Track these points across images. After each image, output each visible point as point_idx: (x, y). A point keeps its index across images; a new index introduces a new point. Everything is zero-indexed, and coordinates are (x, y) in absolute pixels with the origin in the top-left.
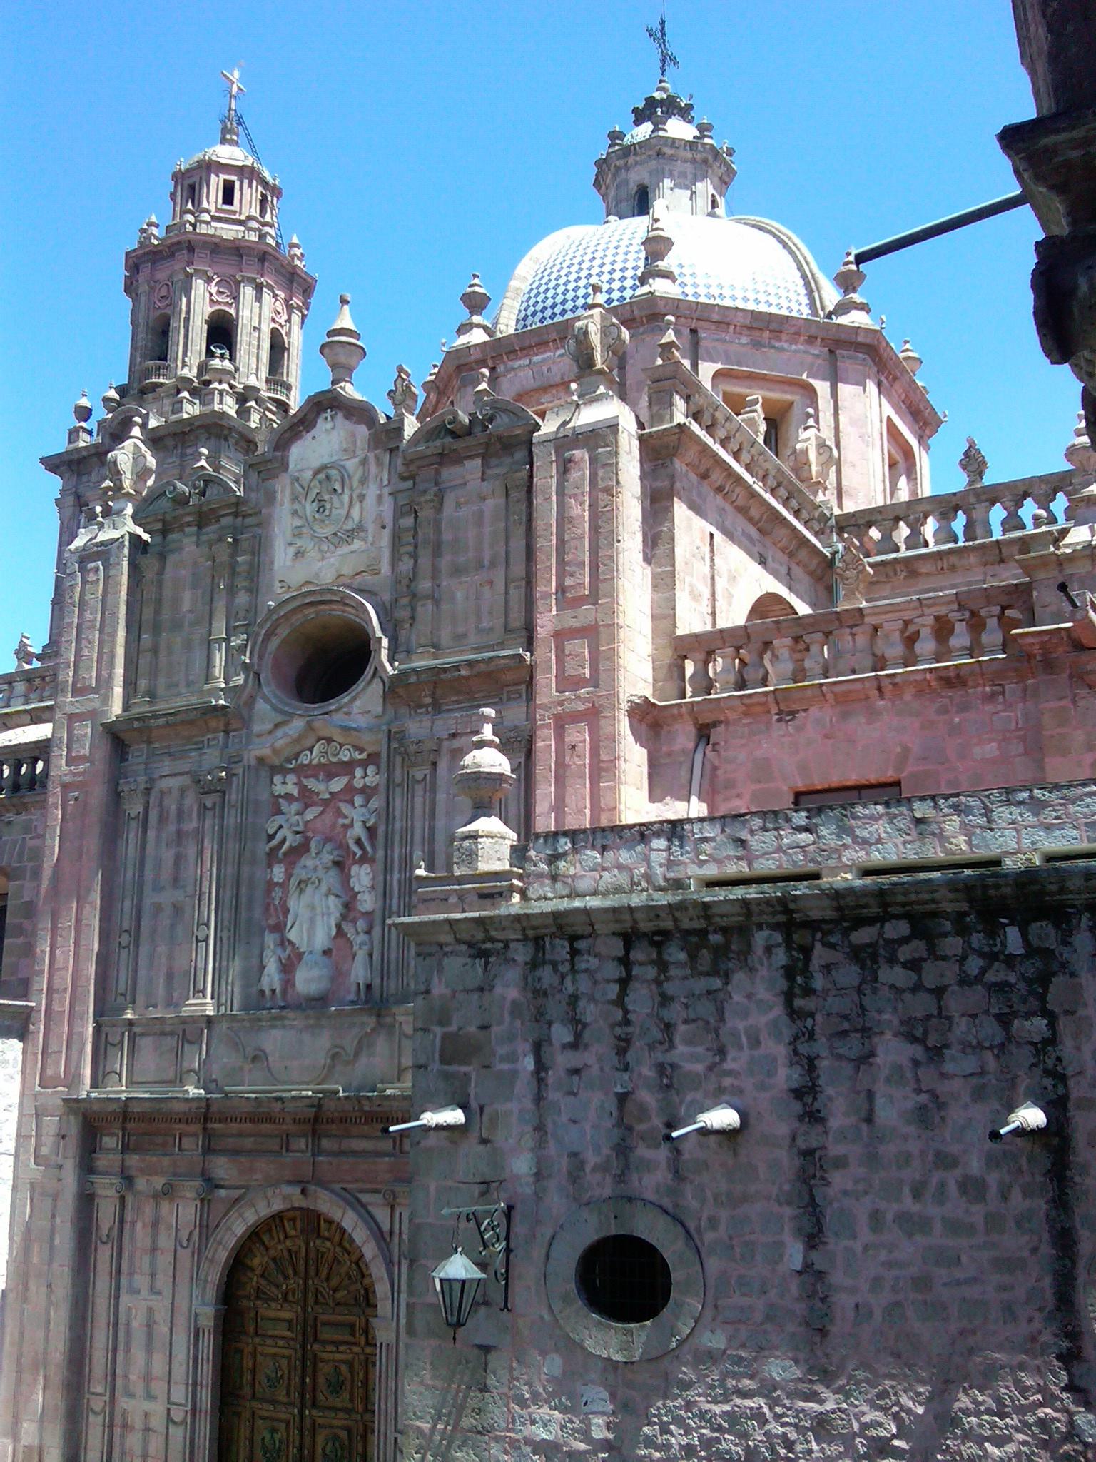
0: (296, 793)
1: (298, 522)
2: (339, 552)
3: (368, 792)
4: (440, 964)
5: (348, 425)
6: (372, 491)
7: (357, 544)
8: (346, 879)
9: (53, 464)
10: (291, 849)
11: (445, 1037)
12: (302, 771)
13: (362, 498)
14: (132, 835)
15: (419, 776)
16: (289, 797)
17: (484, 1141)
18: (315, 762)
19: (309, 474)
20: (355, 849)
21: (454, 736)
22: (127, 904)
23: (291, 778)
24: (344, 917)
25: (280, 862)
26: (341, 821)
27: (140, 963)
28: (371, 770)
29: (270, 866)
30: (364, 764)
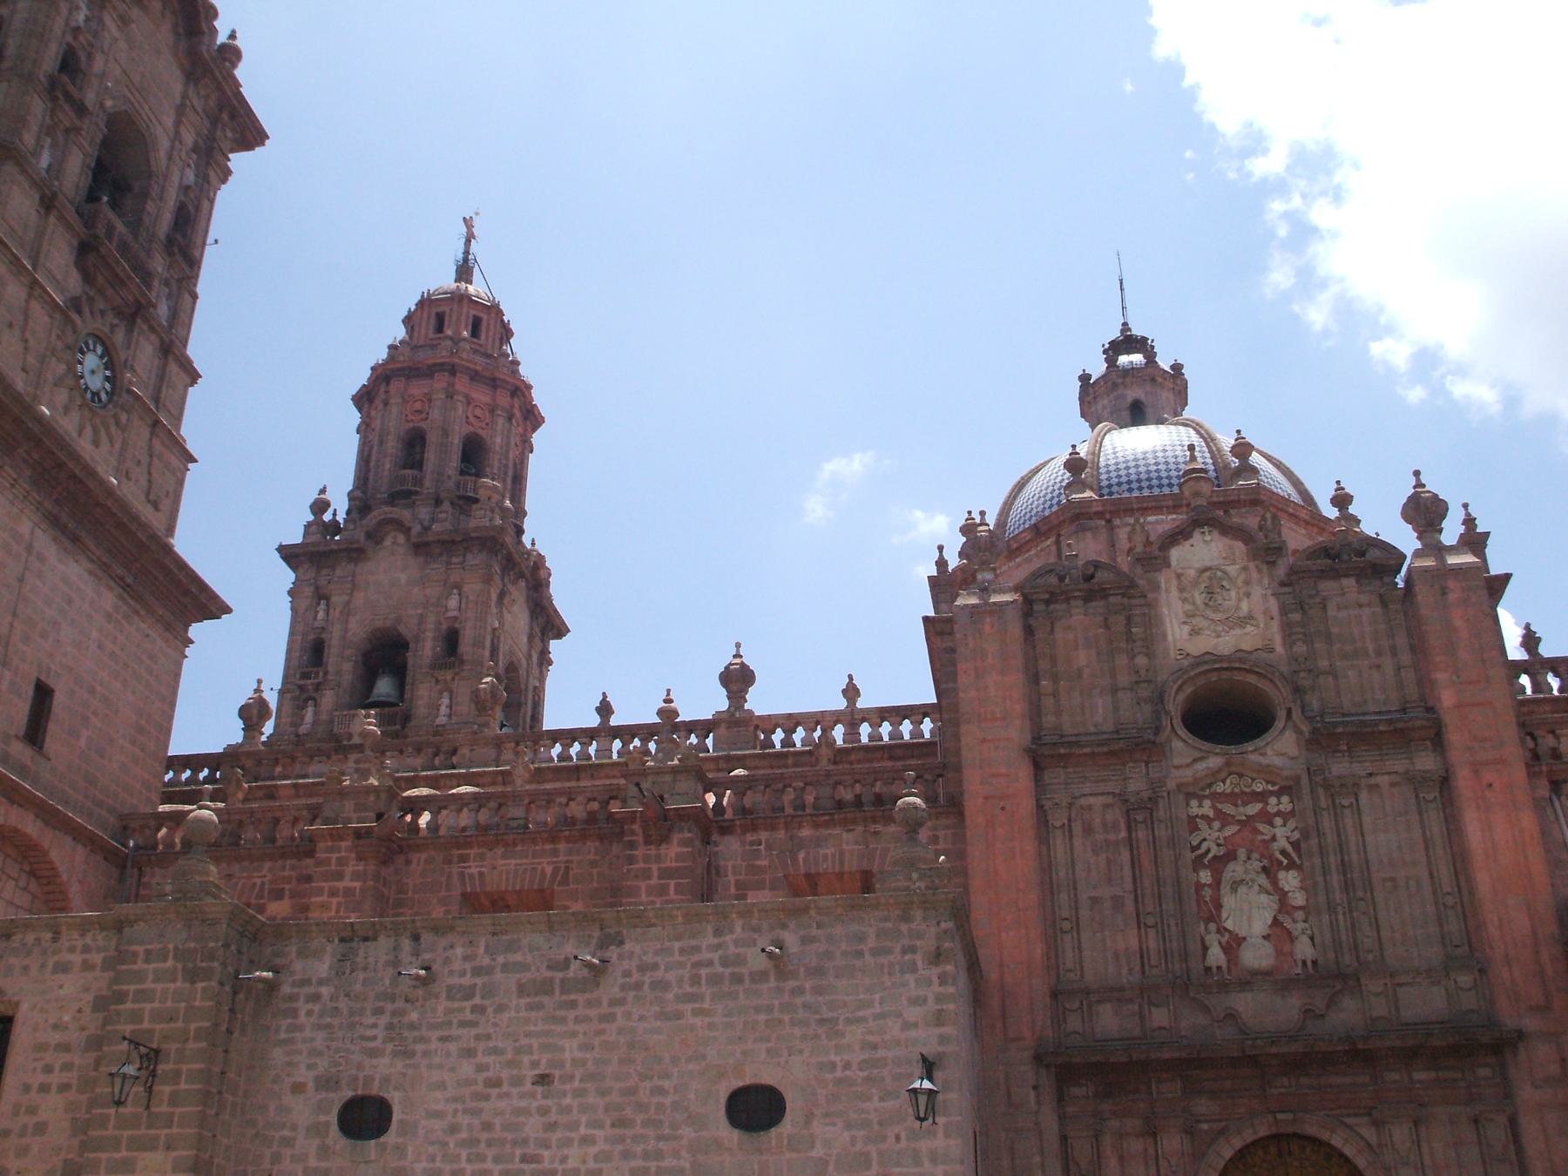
0: (1211, 814)
1: (1188, 607)
2: (1233, 632)
3: (1285, 817)
5: (1226, 541)
6: (1257, 592)
7: (1249, 629)
8: (1274, 882)
9: (289, 554)
10: (1215, 857)
12: (1216, 797)
13: (1248, 595)
14: (1059, 842)
15: (1346, 802)
16: (1203, 817)
18: (1229, 791)
19: (1192, 572)
20: (1280, 857)
22: (1064, 896)
24: (1280, 911)
25: (1205, 867)
26: (1260, 837)
27: (1084, 946)
28: (1285, 799)
29: (1196, 871)
30: (1278, 794)
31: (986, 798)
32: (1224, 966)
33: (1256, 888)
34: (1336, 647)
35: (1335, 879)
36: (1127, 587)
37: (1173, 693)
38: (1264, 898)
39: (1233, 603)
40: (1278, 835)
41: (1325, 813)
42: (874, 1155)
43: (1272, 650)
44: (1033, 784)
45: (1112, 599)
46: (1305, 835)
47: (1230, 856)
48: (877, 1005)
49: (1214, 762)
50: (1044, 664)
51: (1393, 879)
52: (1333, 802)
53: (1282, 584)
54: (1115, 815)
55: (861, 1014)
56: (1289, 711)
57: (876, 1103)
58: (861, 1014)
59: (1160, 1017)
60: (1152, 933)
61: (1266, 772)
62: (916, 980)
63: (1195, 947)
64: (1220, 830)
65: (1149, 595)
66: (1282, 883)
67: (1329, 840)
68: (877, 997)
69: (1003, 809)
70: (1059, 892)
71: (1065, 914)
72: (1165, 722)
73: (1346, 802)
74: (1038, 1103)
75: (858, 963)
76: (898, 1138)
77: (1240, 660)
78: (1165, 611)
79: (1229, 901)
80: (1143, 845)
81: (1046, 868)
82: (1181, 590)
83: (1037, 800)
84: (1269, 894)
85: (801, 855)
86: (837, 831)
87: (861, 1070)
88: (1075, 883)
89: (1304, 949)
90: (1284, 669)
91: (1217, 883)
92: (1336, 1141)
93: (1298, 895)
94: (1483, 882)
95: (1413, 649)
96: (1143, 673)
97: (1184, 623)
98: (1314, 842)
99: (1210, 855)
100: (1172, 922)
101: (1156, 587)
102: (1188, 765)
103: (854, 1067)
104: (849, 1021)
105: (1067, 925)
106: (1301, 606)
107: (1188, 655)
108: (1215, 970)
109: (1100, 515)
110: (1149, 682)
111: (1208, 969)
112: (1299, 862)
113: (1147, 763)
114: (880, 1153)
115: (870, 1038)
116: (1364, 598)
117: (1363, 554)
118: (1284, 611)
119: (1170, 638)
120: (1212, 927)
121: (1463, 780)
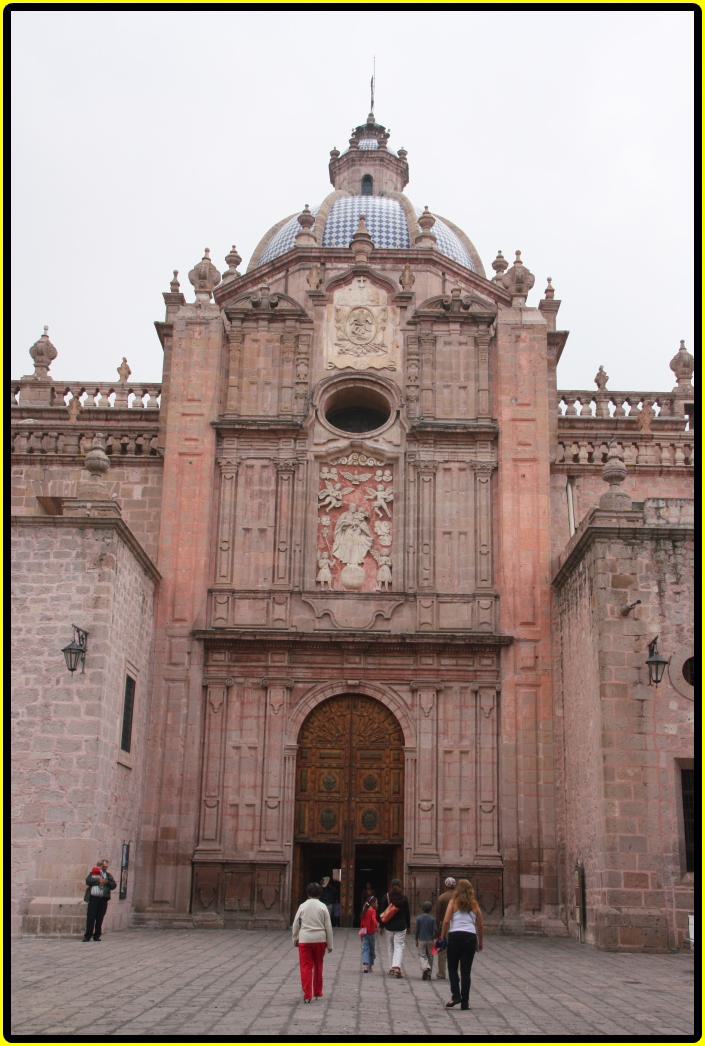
1: (340, 333)
4: (609, 547)
6: (390, 327)
8: (372, 528)
10: (334, 507)
11: (614, 577)
13: (384, 329)
14: (228, 488)
16: (330, 480)
17: (636, 619)
21: (447, 462)
22: (226, 526)
23: (334, 470)
25: (326, 514)
26: (367, 497)
27: (236, 561)
28: (387, 472)
30: (383, 468)
31: (181, 454)
32: (329, 582)
33: (359, 531)
34: (439, 371)
35: (412, 529)
36: (301, 316)
37: (320, 392)
38: (363, 537)
39: (373, 334)
40: (379, 497)
41: (412, 484)
42: (41, 693)
43: (394, 370)
44: (214, 447)
45: (288, 323)
46: (397, 497)
47: (343, 509)
48: (54, 591)
49: (343, 443)
50: (234, 365)
51: (450, 533)
52: (419, 478)
53: (409, 323)
54: (270, 474)
55: (43, 596)
56: (398, 412)
57: (45, 657)
58: (43, 596)
59: (279, 611)
60: (282, 555)
61: (377, 454)
62: (84, 577)
63: (310, 567)
64: (340, 490)
65: (315, 322)
66: (377, 529)
67: (412, 503)
68: (55, 585)
69: (191, 463)
70: (223, 523)
71: (226, 538)
72: (312, 413)
73: (427, 478)
74: (190, 664)
75: (45, 561)
76: (58, 682)
77: (371, 375)
78: (324, 335)
79: (339, 539)
80: (284, 496)
81: (217, 506)
82: (338, 321)
83: (216, 459)
84: (367, 535)
85: (50, 484)
86: (77, 468)
87: (38, 634)
88: (235, 516)
89: (385, 574)
90: (401, 384)
91: (334, 525)
92: (385, 701)
93: (385, 538)
94: (507, 540)
95: (490, 377)
96: (302, 376)
97: (336, 344)
98: (401, 503)
99: (331, 506)
100: (298, 549)
101: (320, 317)
102: (324, 444)
103: (34, 632)
104: (35, 601)
105: (225, 546)
106: (419, 340)
107: (335, 367)
108: (322, 583)
109: (317, 259)
110: (306, 383)
111: (318, 583)
112: (390, 516)
113: (295, 440)
114: (46, 690)
115: (48, 613)
116: (463, 339)
117: (467, 307)
118: (407, 343)
119: (325, 354)
120: (325, 554)
121: (507, 470)
